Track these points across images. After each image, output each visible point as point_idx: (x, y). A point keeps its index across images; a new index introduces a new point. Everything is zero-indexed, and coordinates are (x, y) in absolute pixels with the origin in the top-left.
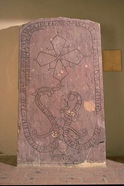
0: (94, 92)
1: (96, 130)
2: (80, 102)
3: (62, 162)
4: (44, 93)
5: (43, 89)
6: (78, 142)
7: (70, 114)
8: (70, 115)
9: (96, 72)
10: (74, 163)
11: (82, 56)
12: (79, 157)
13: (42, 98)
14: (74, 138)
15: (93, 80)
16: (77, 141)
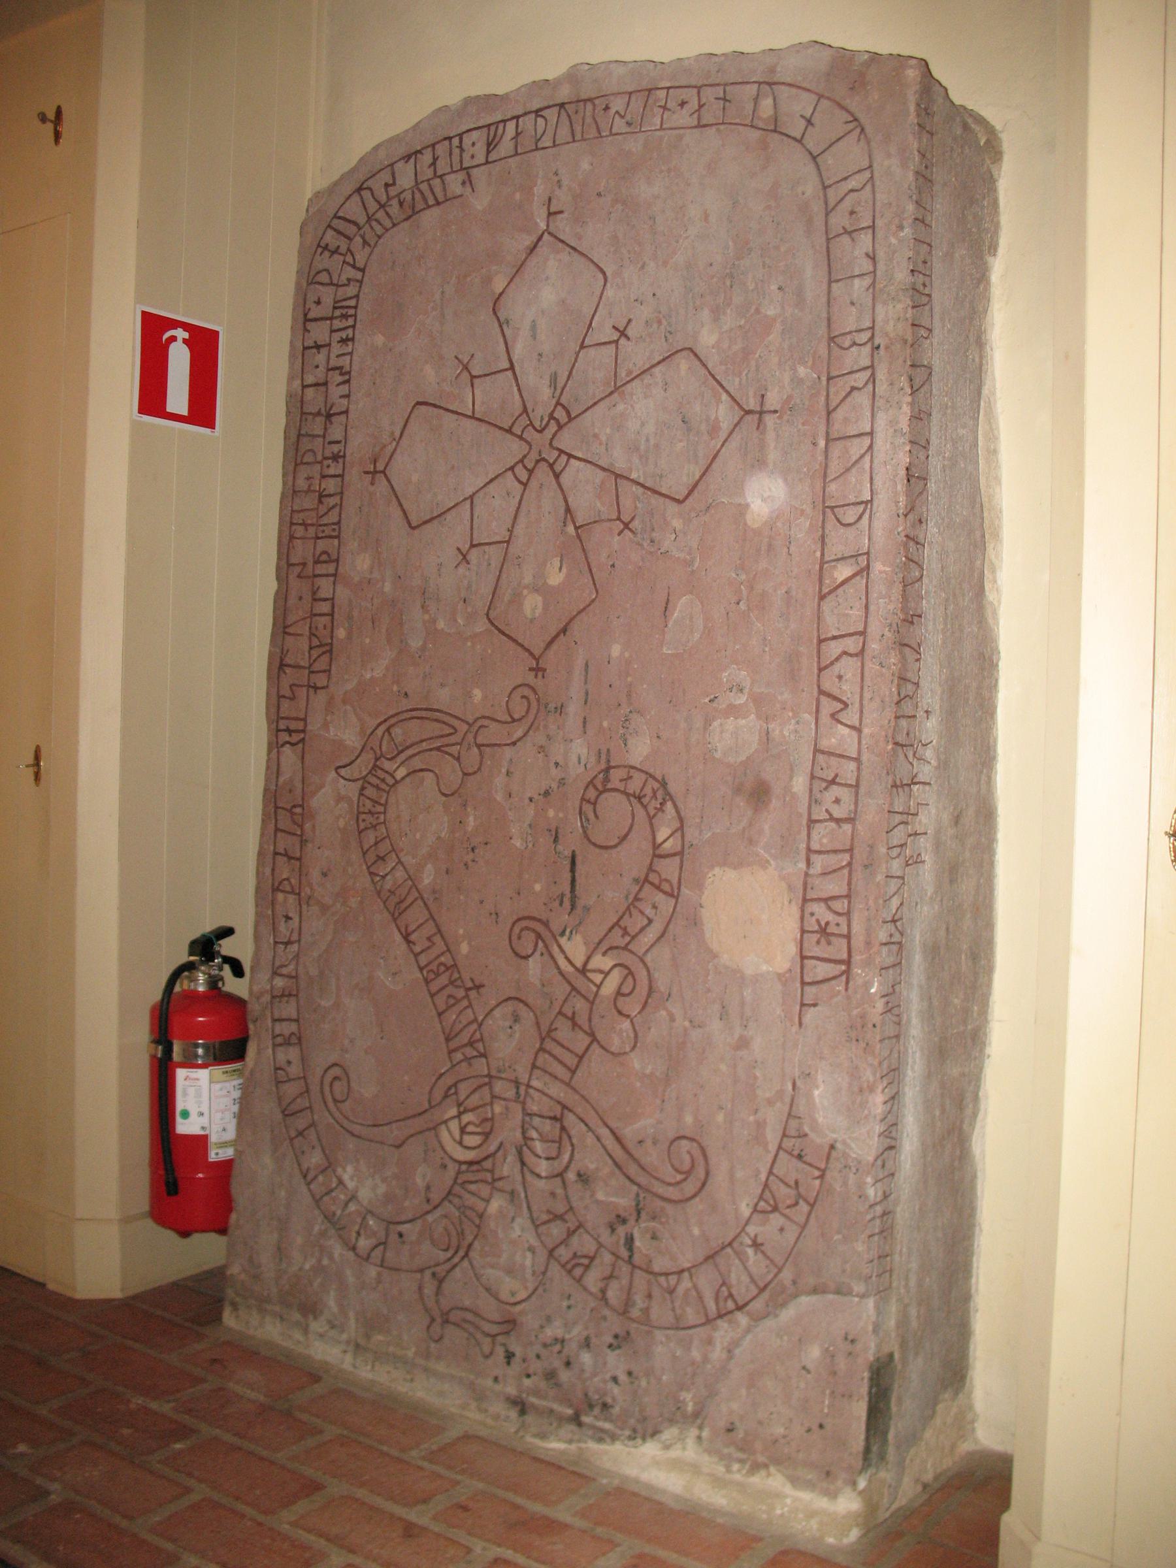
0: (800, 784)
1: (787, 1167)
2: (668, 869)
3: (498, 1387)
4: (417, 763)
5: (415, 730)
6: (630, 1241)
7: (583, 971)
8: (580, 982)
9: (843, 572)
10: (580, 1424)
11: (724, 414)
12: (623, 1377)
13: (402, 802)
14: (600, 1196)
15: (808, 665)
16: (621, 1230)
